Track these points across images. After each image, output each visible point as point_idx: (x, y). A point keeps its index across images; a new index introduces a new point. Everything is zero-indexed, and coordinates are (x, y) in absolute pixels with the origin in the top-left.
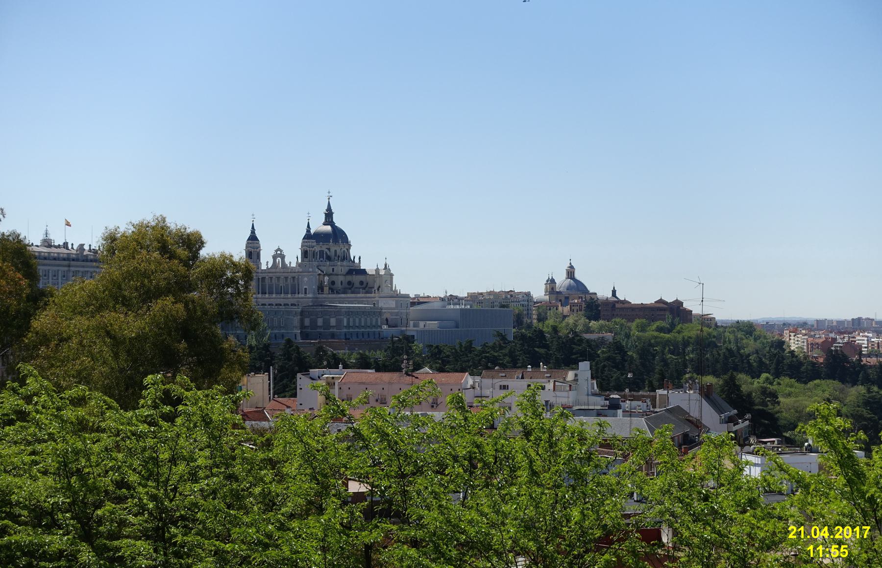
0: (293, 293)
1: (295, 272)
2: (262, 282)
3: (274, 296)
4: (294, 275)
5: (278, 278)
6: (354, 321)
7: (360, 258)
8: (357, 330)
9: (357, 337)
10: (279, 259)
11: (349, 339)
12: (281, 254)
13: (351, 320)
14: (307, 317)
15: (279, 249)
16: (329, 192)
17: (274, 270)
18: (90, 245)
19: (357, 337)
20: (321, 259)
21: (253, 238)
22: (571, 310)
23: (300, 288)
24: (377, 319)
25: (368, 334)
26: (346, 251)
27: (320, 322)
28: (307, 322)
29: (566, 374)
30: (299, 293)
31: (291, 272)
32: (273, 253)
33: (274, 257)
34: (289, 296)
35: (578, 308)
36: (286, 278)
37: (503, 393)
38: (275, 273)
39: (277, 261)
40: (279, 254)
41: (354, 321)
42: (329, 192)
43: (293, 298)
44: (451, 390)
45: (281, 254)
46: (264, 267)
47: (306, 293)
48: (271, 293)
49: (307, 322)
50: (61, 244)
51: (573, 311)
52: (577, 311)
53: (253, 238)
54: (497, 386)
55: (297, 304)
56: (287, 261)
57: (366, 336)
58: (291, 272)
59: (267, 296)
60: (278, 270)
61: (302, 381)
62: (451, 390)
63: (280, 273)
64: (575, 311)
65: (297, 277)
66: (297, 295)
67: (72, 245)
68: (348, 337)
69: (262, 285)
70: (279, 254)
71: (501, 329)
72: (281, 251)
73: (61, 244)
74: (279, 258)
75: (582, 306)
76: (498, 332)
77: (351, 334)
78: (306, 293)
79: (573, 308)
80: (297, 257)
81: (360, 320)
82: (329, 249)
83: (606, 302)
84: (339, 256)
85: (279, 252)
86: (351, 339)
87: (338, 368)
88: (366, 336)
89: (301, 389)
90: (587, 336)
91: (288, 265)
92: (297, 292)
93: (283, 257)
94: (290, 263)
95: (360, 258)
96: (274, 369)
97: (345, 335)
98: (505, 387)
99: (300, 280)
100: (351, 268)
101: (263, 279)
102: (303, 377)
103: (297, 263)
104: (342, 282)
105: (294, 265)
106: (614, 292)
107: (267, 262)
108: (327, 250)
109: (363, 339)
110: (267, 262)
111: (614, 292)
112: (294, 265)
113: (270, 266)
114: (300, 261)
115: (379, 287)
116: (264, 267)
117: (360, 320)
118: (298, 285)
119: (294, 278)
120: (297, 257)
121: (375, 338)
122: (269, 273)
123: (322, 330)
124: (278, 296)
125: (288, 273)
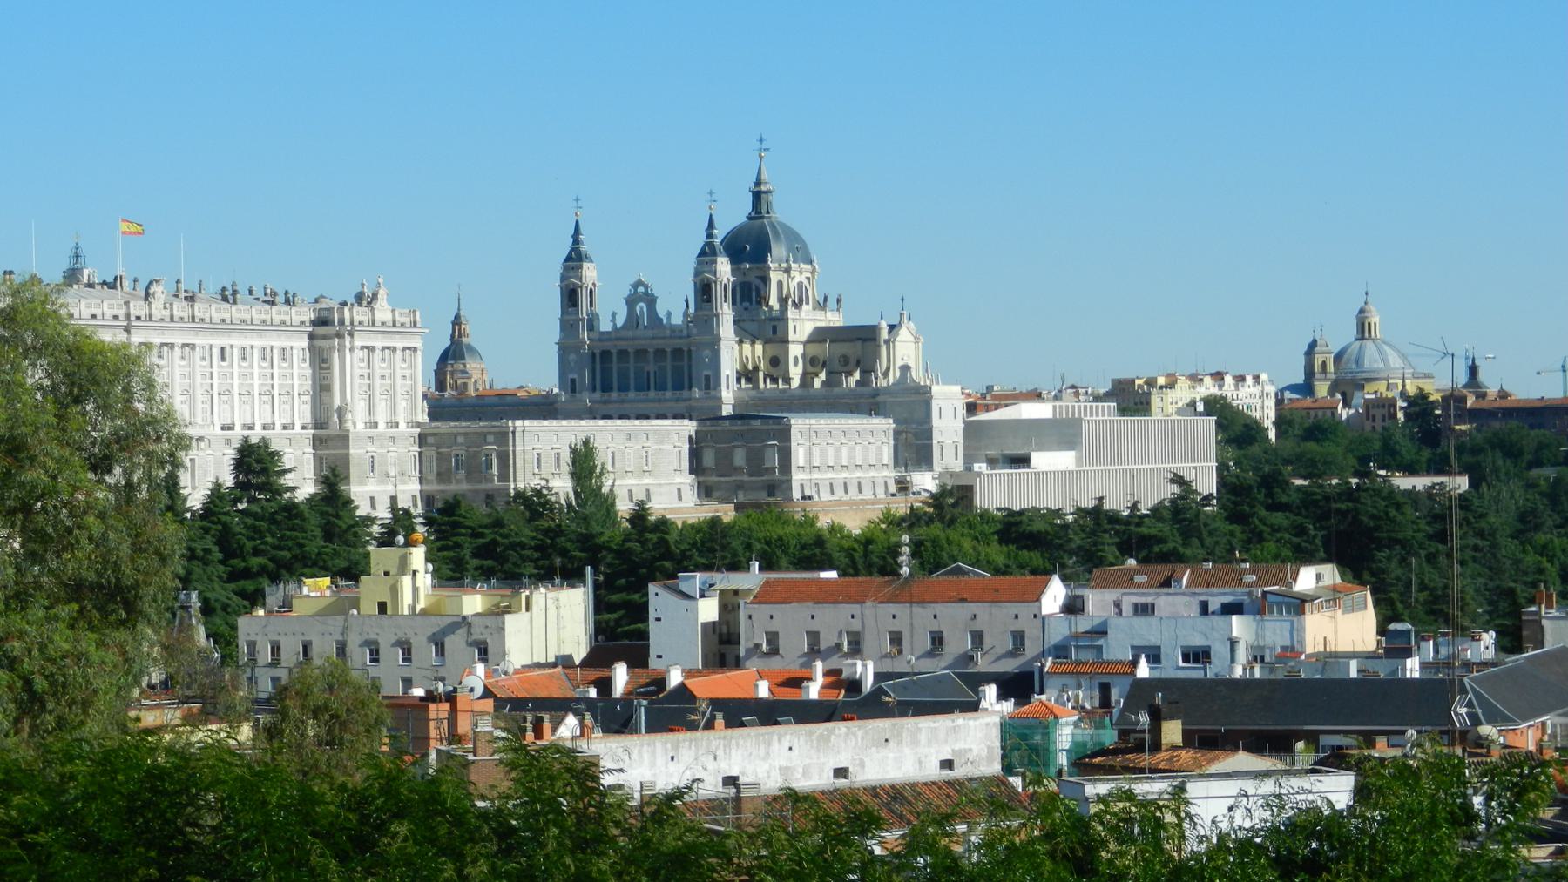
0: (678, 386)
1: (681, 338)
2: (602, 362)
3: (632, 395)
4: (678, 343)
5: (641, 353)
6: (823, 454)
7: (839, 301)
8: (830, 475)
9: (832, 492)
10: (641, 307)
11: (810, 498)
12: (646, 293)
13: (816, 451)
14: (707, 447)
15: (639, 283)
16: (761, 140)
17: (630, 334)
18: (178, 282)
19: (832, 492)
20: (746, 304)
21: (575, 259)
22: (1368, 418)
23: (694, 375)
24: (879, 448)
25: (859, 484)
26: (805, 282)
27: (739, 458)
28: (709, 459)
29: (1295, 576)
30: (690, 388)
31: (671, 337)
32: (626, 291)
33: (631, 302)
34: (669, 394)
35: (1385, 411)
36: (660, 353)
37: (1141, 622)
38: (633, 339)
39: (638, 310)
40: (641, 296)
41: (823, 454)
42: (761, 140)
43: (677, 400)
44: (1017, 617)
45: (646, 293)
46: (605, 326)
47: (708, 387)
48: (623, 388)
49: (709, 459)
50: (110, 280)
51: (1374, 420)
52: (1384, 420)
53: (575, 259)
54: (1127, 608)
55: (687, 415)
56: (661, 311)
57: (853, 490)
58: (671, 337)
59: (614, 395)
60: (640, 332)
61: (659, 598)
62: (1017, 617)
63: (645, 339)
64: (1379, 418)
65: (686, 349)
66: (685, 393)
67: (135, 281)
68: (807, 493)
69: (603, 370)
70: (641, 296)
71: (1185, 468)
72: (646, 287)
73: (110, 280)
74: (642, 304)
75: (1395, 406)
76: (1175, 474)
77: (817, 485)
78: (708, 387)
79: (1371, 412)
80: (687, 301)
81: (838, 451)
82: (765, 280)
83: (1453, 399)
84: (788, 296)
85: (641, 289)
86: (816, 498)
87: (748, 569)
88: (853, 490)
89: (658, 619)
90: (1403, 482)
91: (665, 321)
92: (686, 385)
93: (651, 301)
94: (669, 314)
95: (839, 301)
96: (596, 572)
97: (802, 486)
98: (1144, 610)
99: (694, 356)
100: (822, 324)
101: (606, 355)
102: (660, 592)
103: (686, 314)
104: (796, 359)
105: (677, 319)
106: (1473, 370)
107: (614, 315)
108: (758, 282)
109: (846, 498)
110: (614, 315)
111: (1473, 370)
112: (677, 319)
113: (619, 325)
114: (692, 310)
115: (888, 369)
116: (605, 326)
117: (838, 451)
118: (690, 367)
119: (677, 353)
120: (687, 301)
121: (875, 494)
122: (618, 339)
123: (746, 478)
124: (642, 395)
125: (664, 338)
